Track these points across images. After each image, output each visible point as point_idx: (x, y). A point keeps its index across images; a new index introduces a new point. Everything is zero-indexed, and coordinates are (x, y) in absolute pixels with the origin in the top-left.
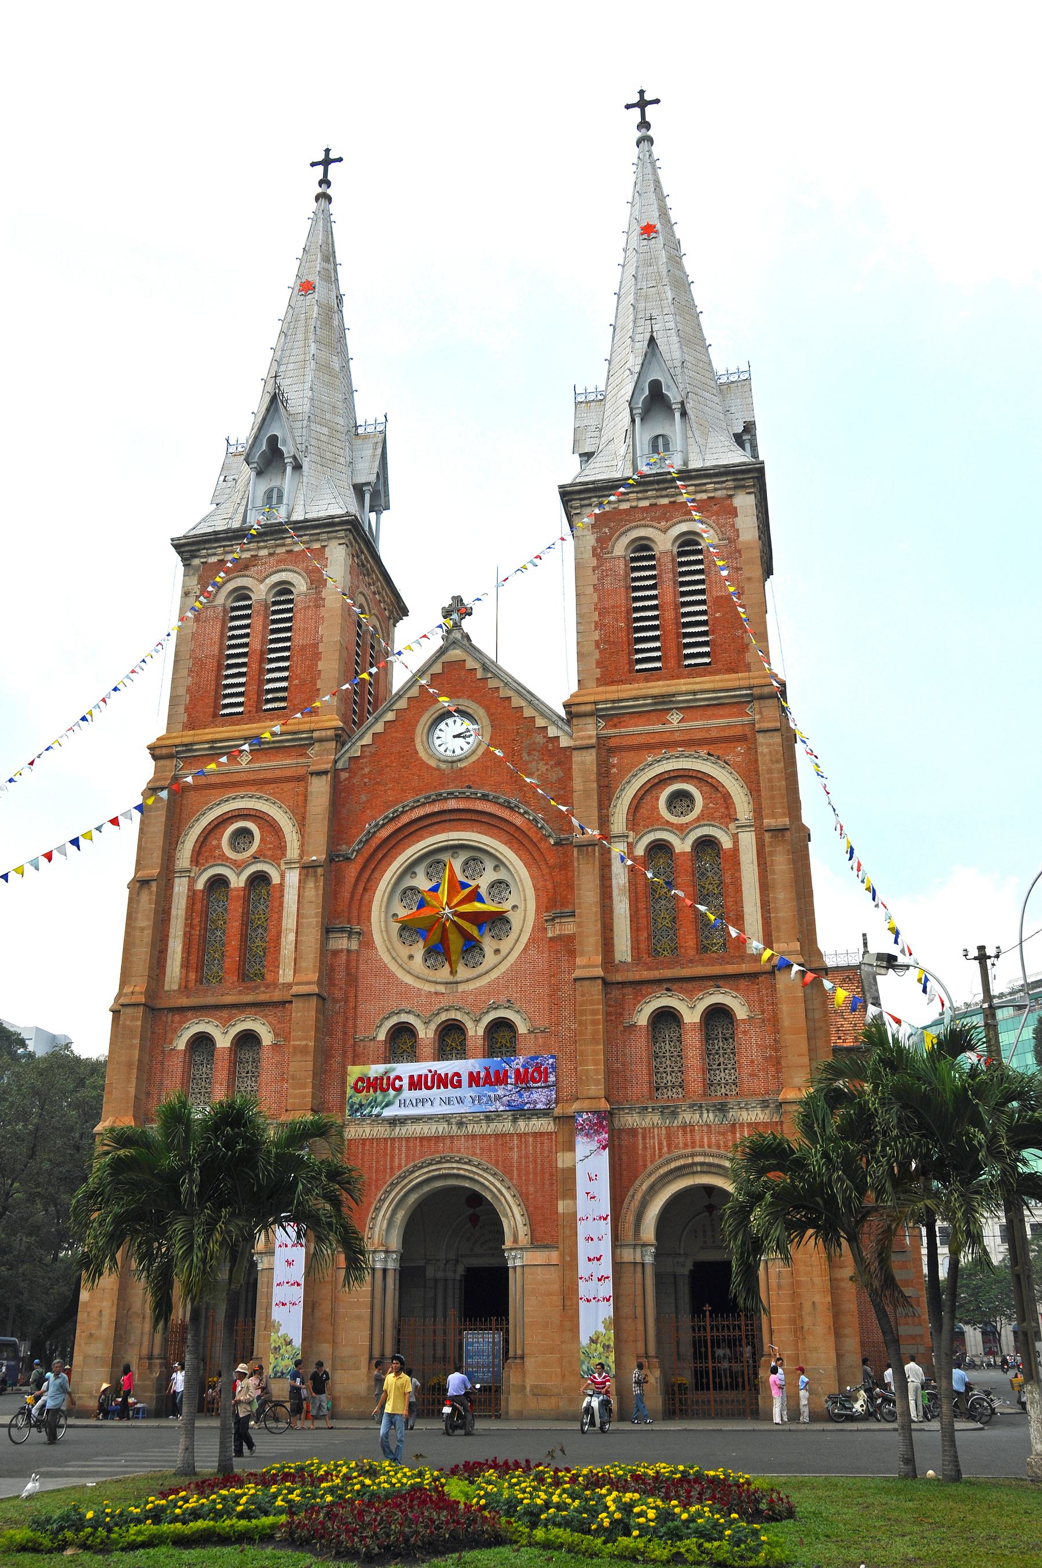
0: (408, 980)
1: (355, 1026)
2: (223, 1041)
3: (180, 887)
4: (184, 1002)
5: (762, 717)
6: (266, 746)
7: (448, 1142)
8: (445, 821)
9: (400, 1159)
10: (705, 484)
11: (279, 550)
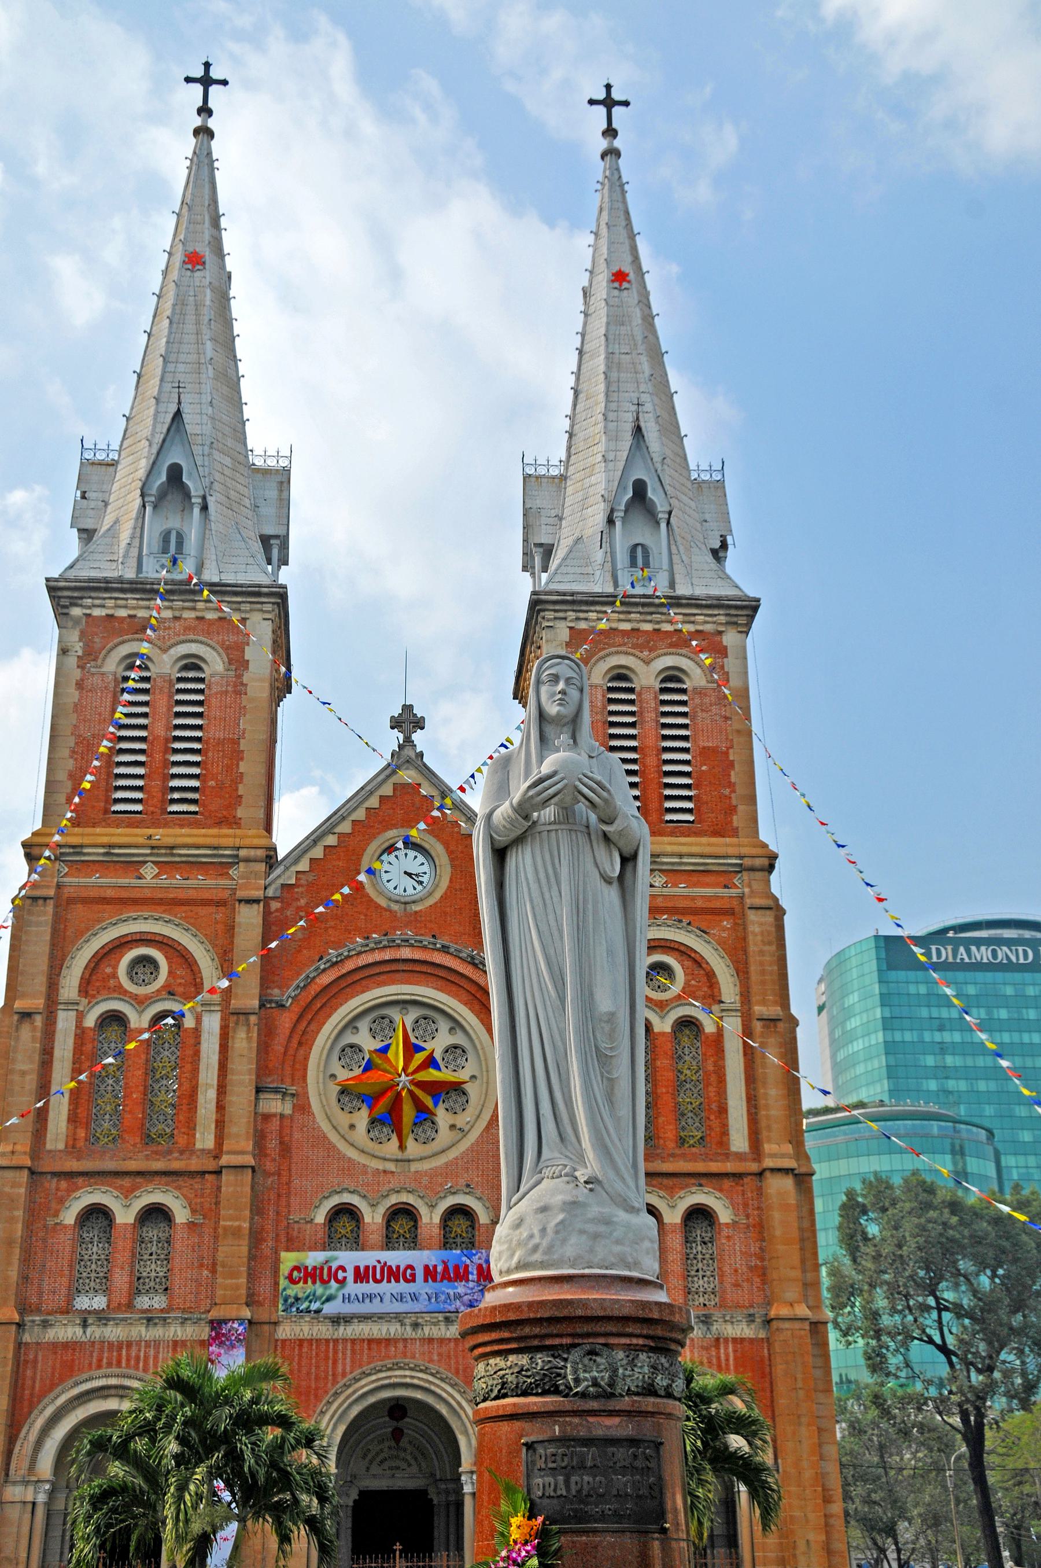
0: (352, 1153)
1: (288, 1205)
2: (125, 1215)
3: (65, 1022)
4: (73, 1165)
5: (752, 892)
6: (177, 859)
7: (401, 1345)
8: (398, 971)
9: (344, 1365)
10: (695, 615)
11: (187, 614)
